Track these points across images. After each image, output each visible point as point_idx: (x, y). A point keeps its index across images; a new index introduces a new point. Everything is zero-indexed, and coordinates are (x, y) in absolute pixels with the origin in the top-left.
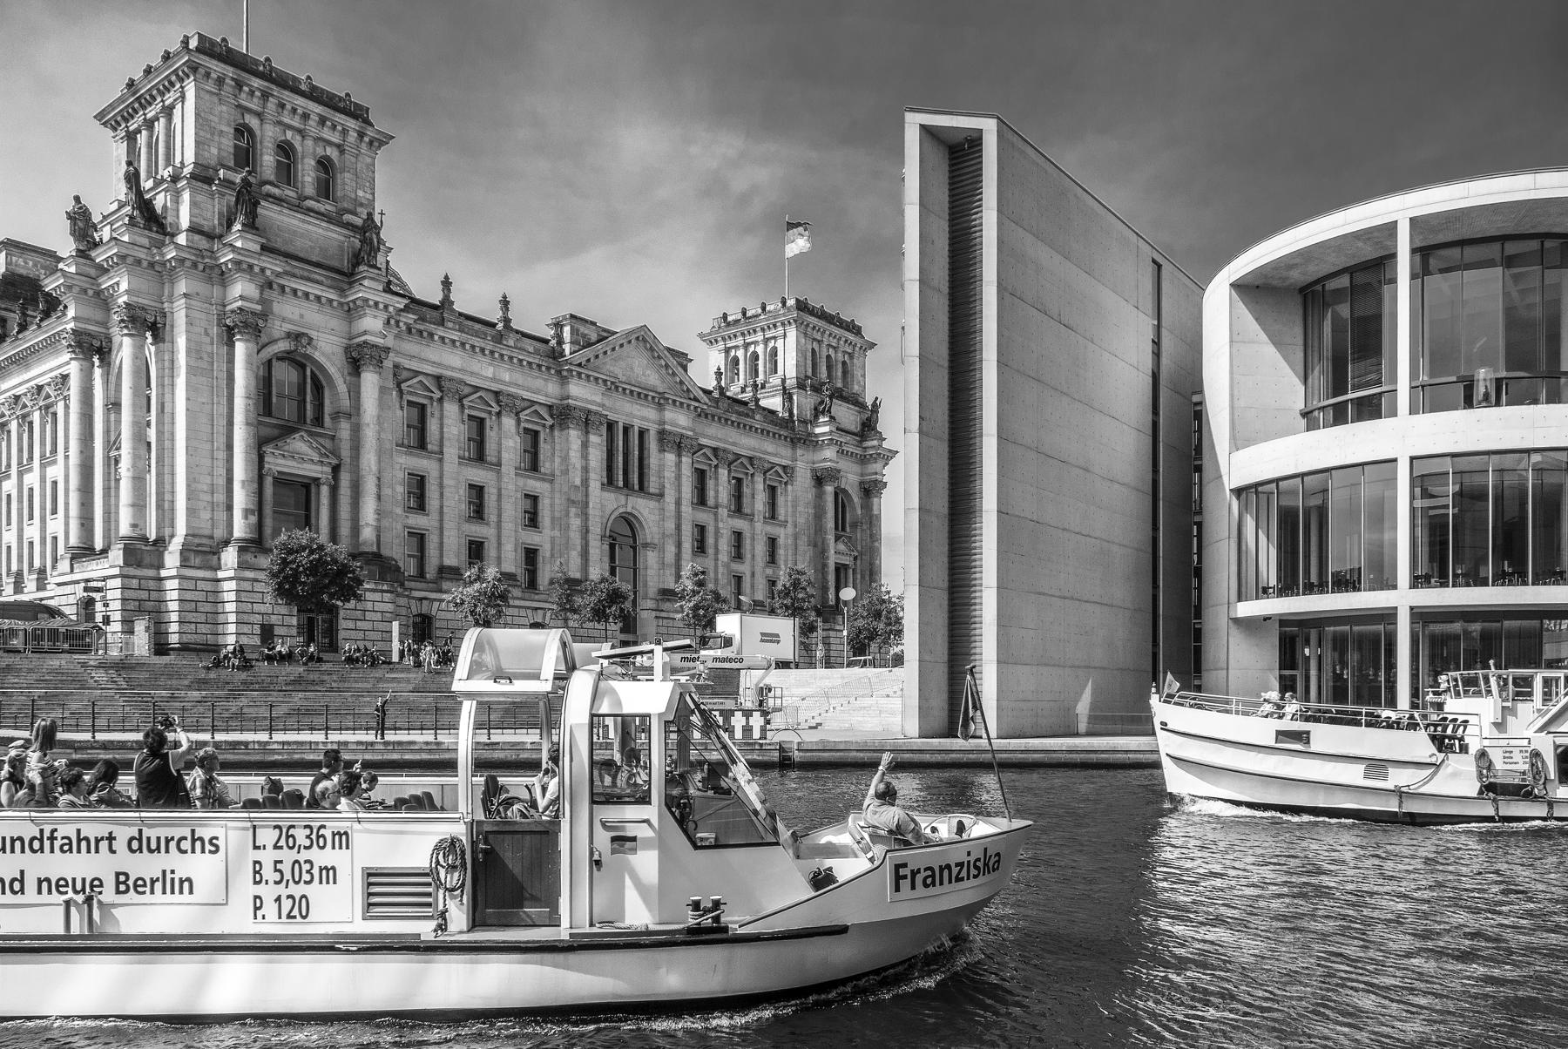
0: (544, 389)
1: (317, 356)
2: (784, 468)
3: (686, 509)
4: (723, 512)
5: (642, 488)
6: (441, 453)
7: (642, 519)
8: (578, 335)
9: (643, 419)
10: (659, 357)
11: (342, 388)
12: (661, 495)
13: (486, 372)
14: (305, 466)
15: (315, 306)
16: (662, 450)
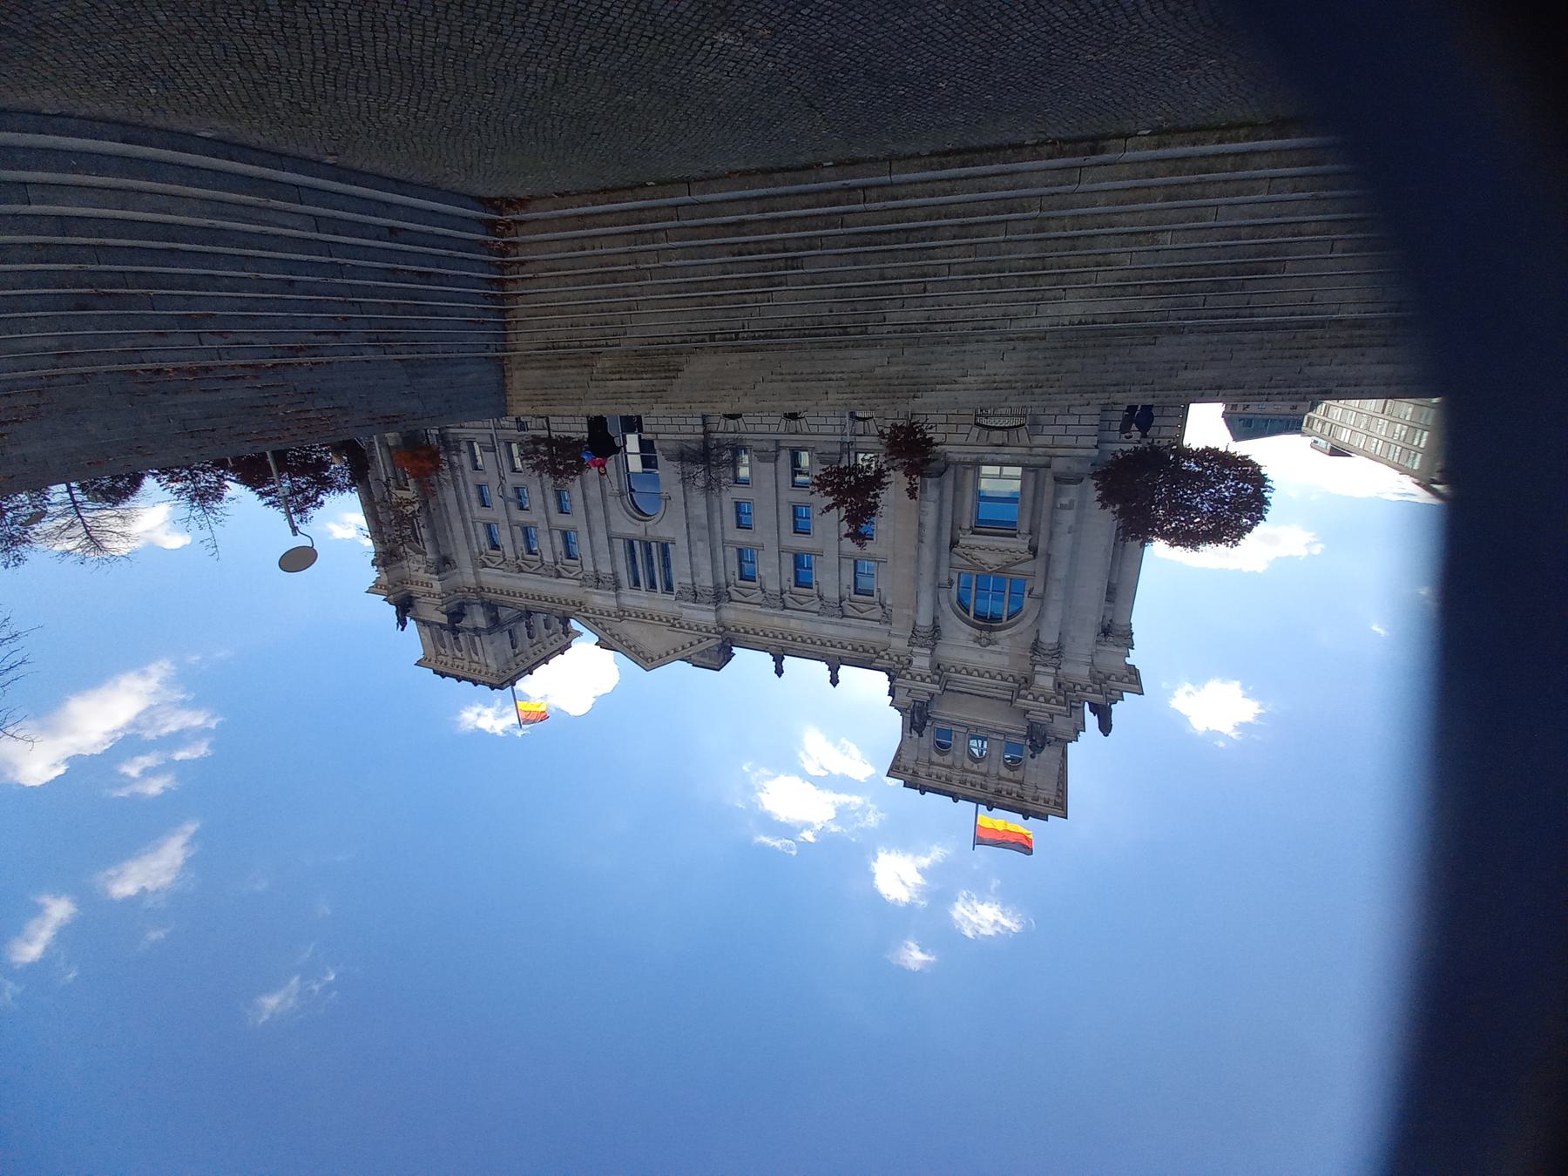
0: (733, 614)
1: (969, 629)
2: (485, 566)
3: (583, 530)
4: (543, 526)
5: (631, 543)
6: (839, 558)
7: (629, 517)
8: (710, 656)
9: (639, 597)
10: (630, 647)
11: (945, 606)
12: (610, 539)
13: (798, 624)
14: (986, 544)
15: (970, 667)
16: (615, 574)
